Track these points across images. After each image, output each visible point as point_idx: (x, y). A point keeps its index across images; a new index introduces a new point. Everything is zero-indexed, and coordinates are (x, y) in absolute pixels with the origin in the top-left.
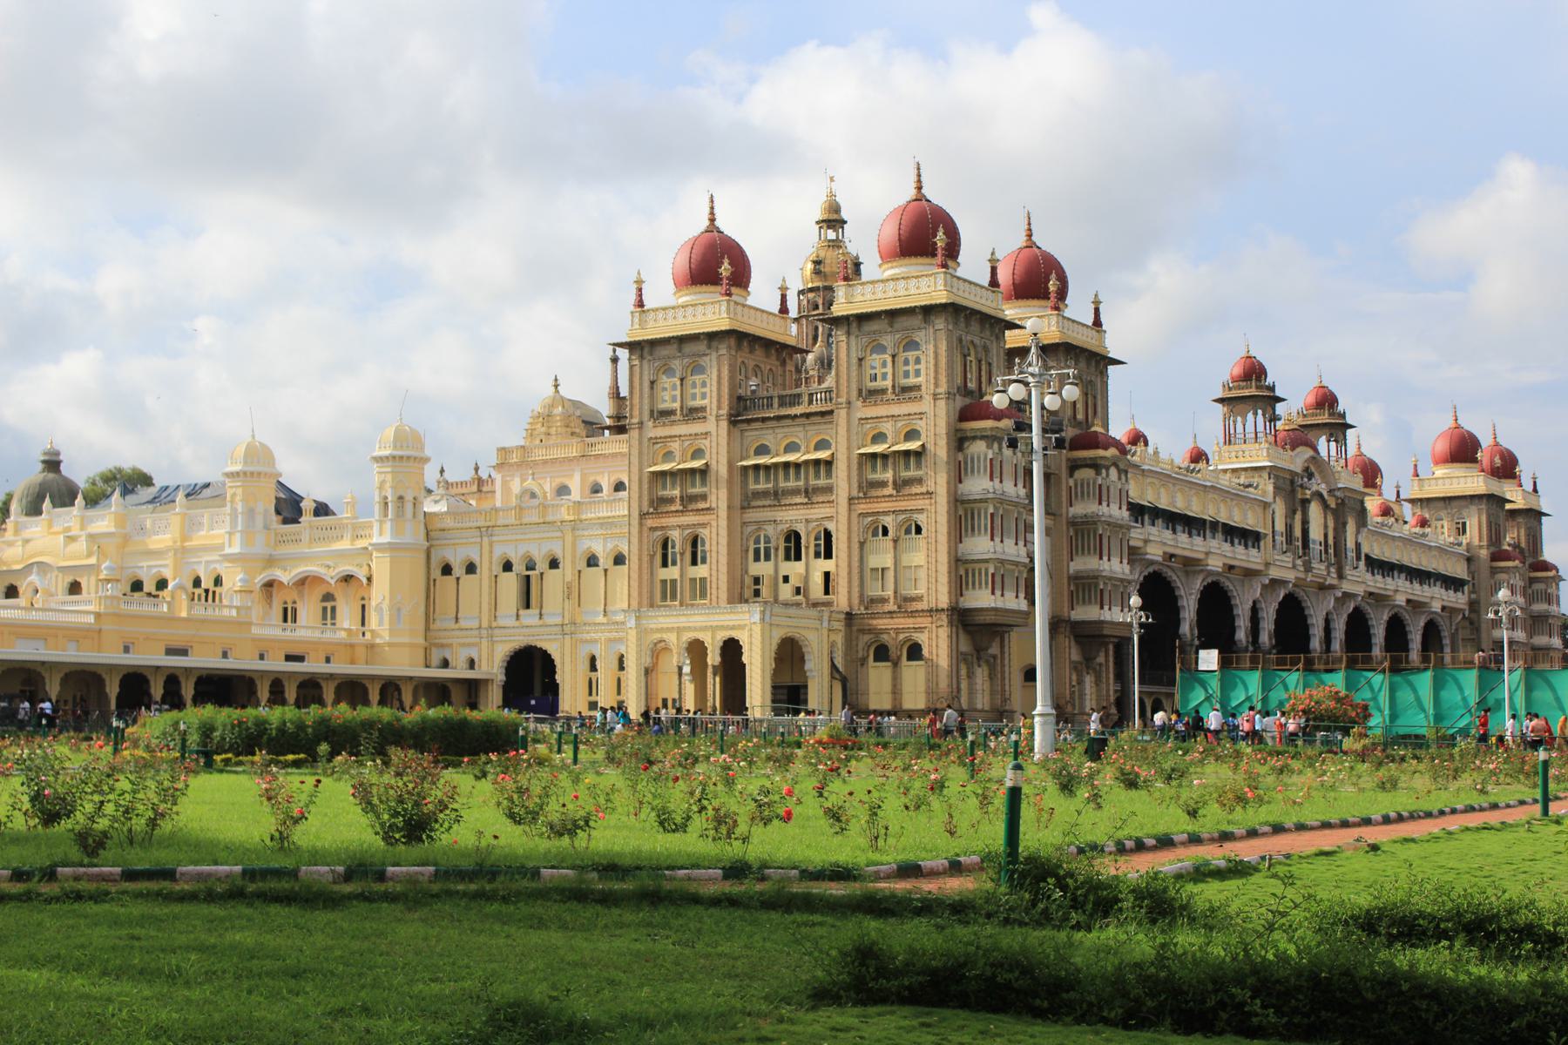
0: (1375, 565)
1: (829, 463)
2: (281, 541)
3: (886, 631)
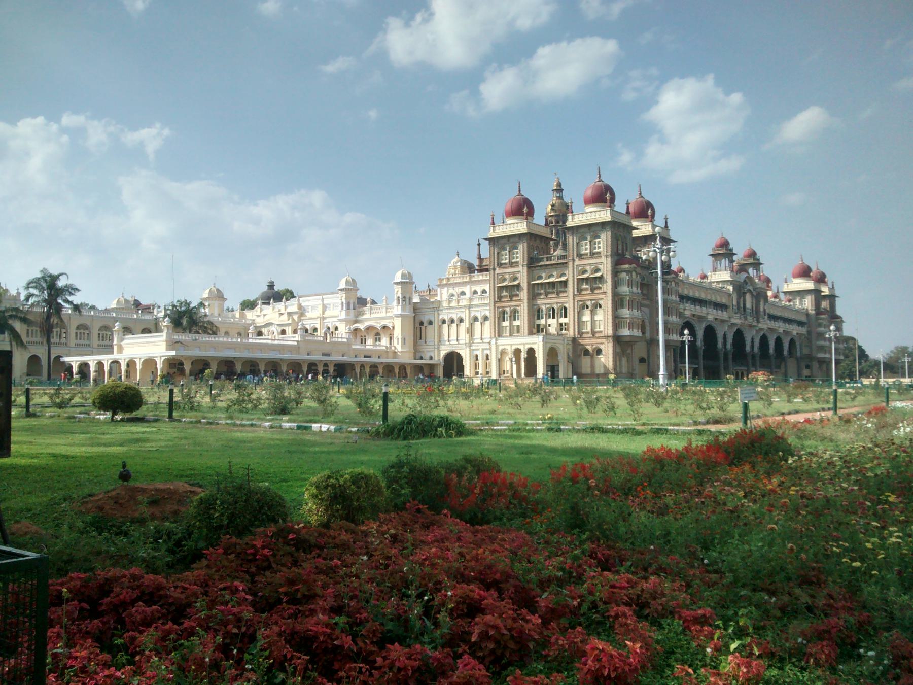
3: (589, 344)
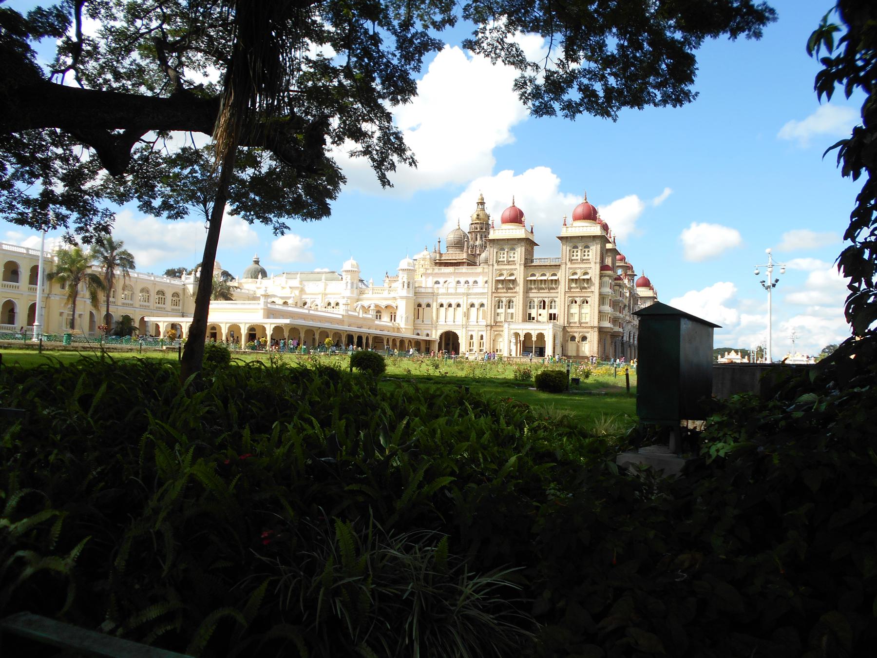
1: (556, 281)
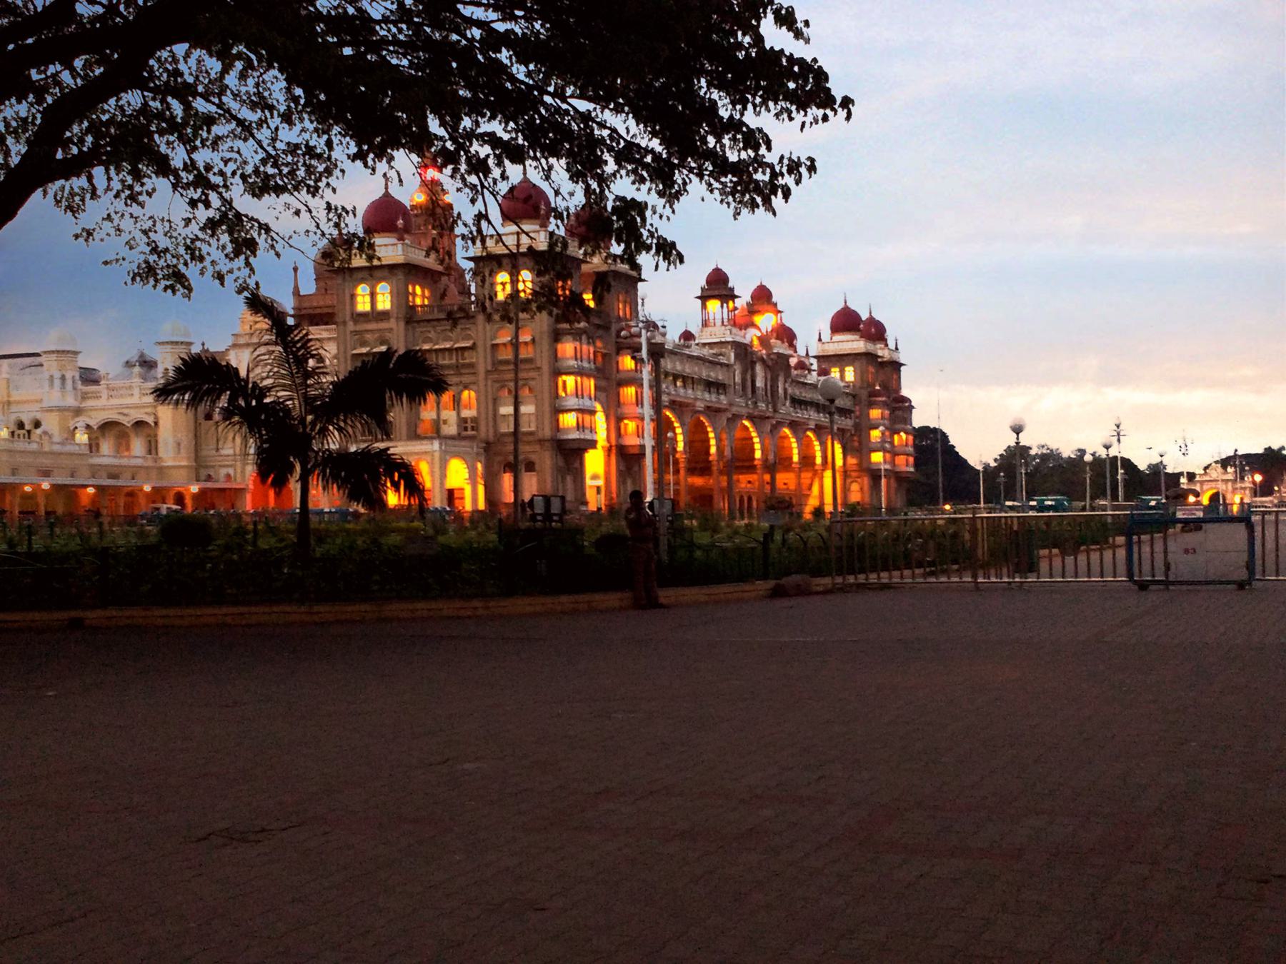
0: (797, 402)
2: (85, 397)
